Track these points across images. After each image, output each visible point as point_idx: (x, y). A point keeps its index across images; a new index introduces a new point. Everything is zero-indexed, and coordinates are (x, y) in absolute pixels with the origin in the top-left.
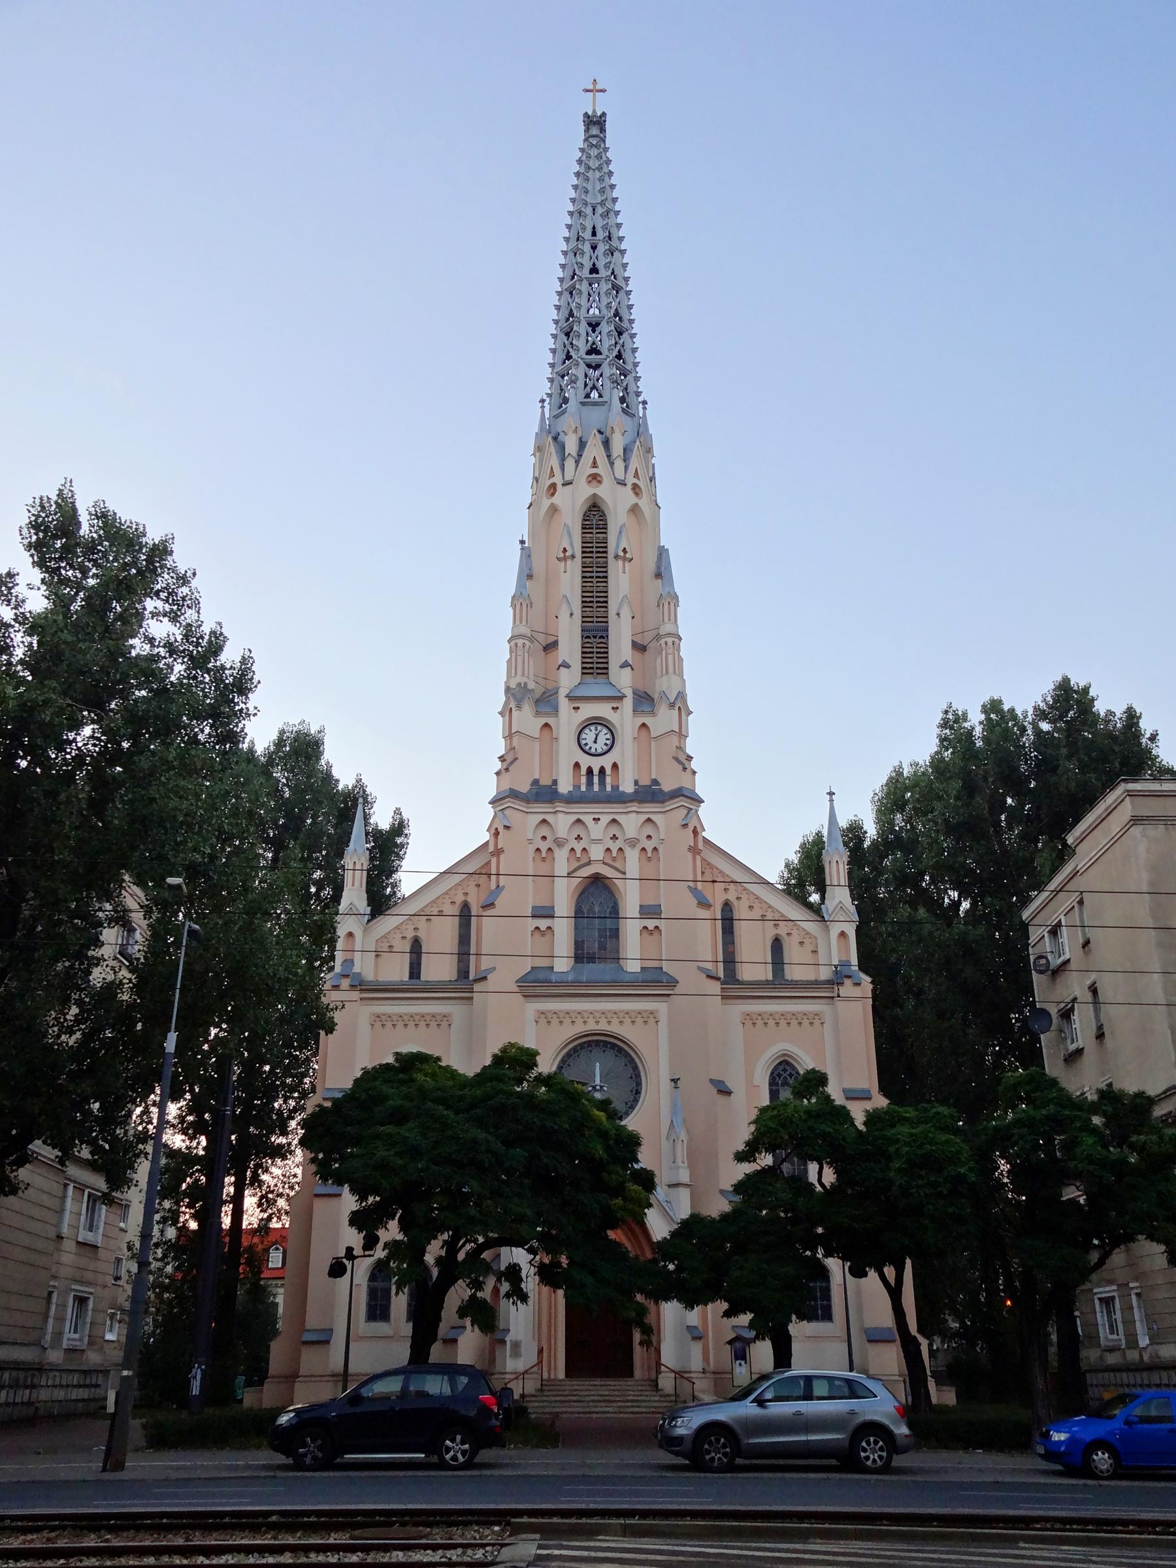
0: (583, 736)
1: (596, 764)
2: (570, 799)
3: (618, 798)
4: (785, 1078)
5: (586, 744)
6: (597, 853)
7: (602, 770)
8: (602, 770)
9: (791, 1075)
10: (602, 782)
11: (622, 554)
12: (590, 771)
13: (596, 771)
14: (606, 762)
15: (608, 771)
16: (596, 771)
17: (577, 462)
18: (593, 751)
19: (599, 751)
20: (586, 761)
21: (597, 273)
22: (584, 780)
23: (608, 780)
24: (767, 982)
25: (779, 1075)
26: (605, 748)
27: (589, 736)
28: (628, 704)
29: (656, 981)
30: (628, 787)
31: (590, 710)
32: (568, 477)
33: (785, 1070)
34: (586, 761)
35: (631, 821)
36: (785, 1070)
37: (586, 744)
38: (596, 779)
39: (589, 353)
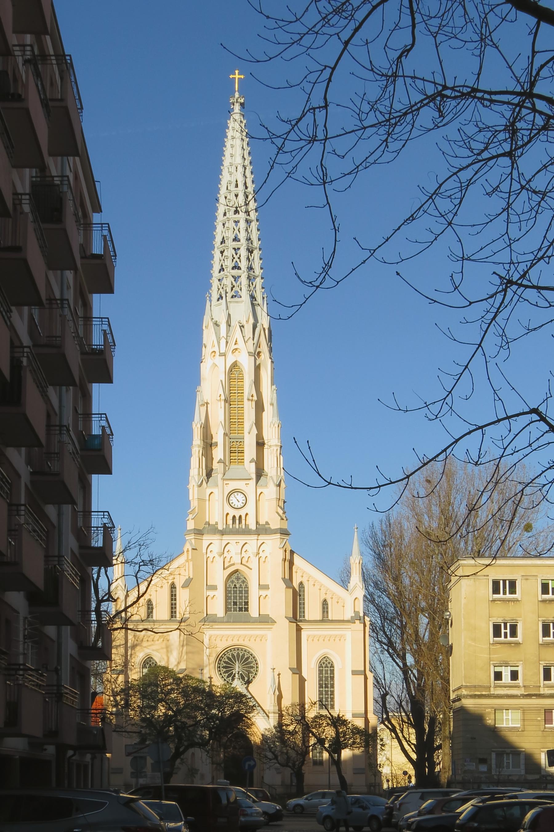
0: (231, 502)
1: (237, 514)
2: (223, 533)
3: (247, 532)
4: (326, 665)
5: (232, 503)
6: (236, 559)
7: (240, 517)
8: (240, 517)
9: (329, 663)
10: (240, 522)
11: (251, 398)
12: (234, 517)
13: (237, 518)
14: (242, 512)
15: (243, 518)
16: (237, 518)
17: (227, 342)
18: (236, 506)
19: (239, 506)
20: (232, 512)
21: (239, 268)
22: (230, 522)
23: (243, 522)
24: (320, 620)
25: (324, 663)
26: (242, 505)
27: (232, 498)
28: (254, 481)
29: (265, 620)
30: (253, 527)
31: (233, 485)
32: (222, 351)
33: (326, 661)
34: (232, 512)
35: (252, 542)
36: (326, 661)
37: (232, 503)
38: (237, 521)
39: (233, 268)
